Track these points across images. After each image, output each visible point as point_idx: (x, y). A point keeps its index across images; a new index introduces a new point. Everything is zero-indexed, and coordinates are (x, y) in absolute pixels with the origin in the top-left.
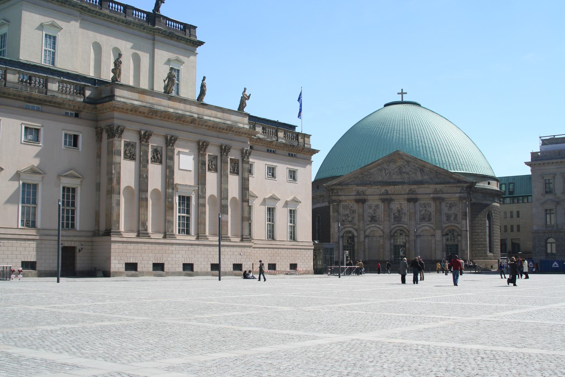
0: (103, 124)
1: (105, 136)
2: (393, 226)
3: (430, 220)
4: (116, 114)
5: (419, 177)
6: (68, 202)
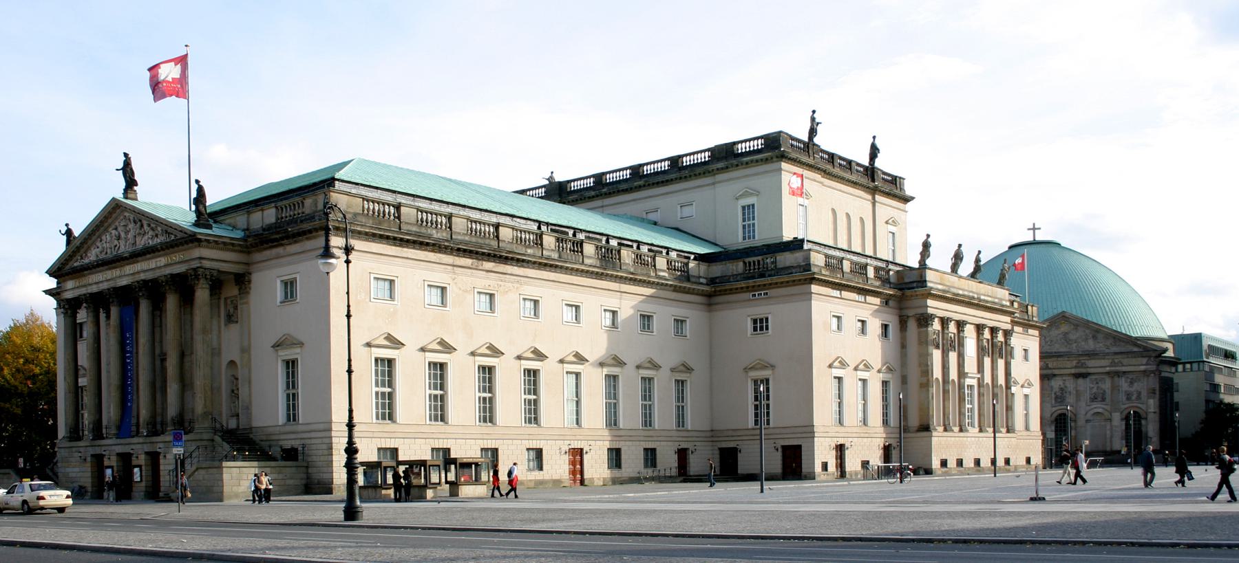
0: (911, 313)
1: (912, 325)
2: (1054, 409)
3: (1103, 400)
4: (930, 302)
5: (1091, 345)
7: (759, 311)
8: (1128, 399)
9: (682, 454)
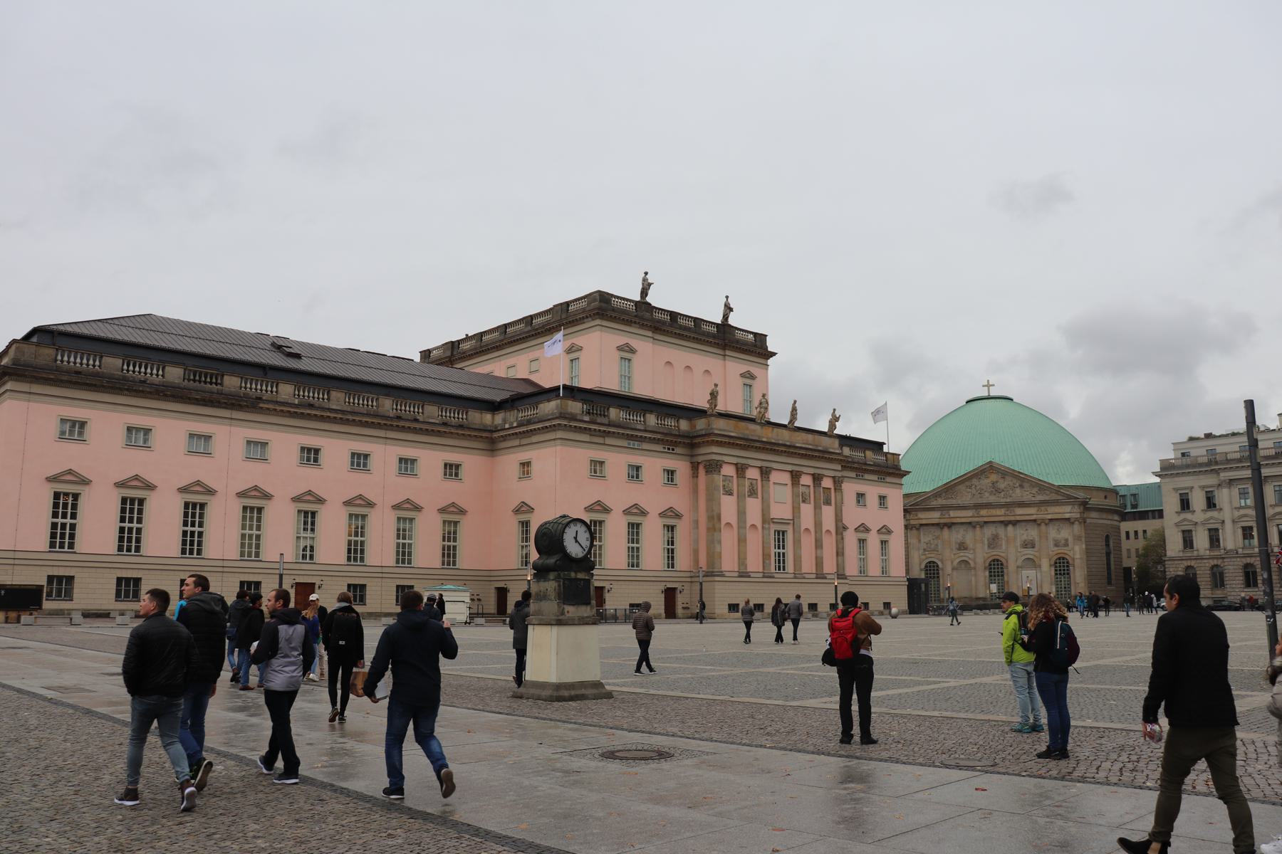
1: (702, 471)
5: (1018, 494)
7: (524, 455)
8: (1056, 545)
9: (670, 594)
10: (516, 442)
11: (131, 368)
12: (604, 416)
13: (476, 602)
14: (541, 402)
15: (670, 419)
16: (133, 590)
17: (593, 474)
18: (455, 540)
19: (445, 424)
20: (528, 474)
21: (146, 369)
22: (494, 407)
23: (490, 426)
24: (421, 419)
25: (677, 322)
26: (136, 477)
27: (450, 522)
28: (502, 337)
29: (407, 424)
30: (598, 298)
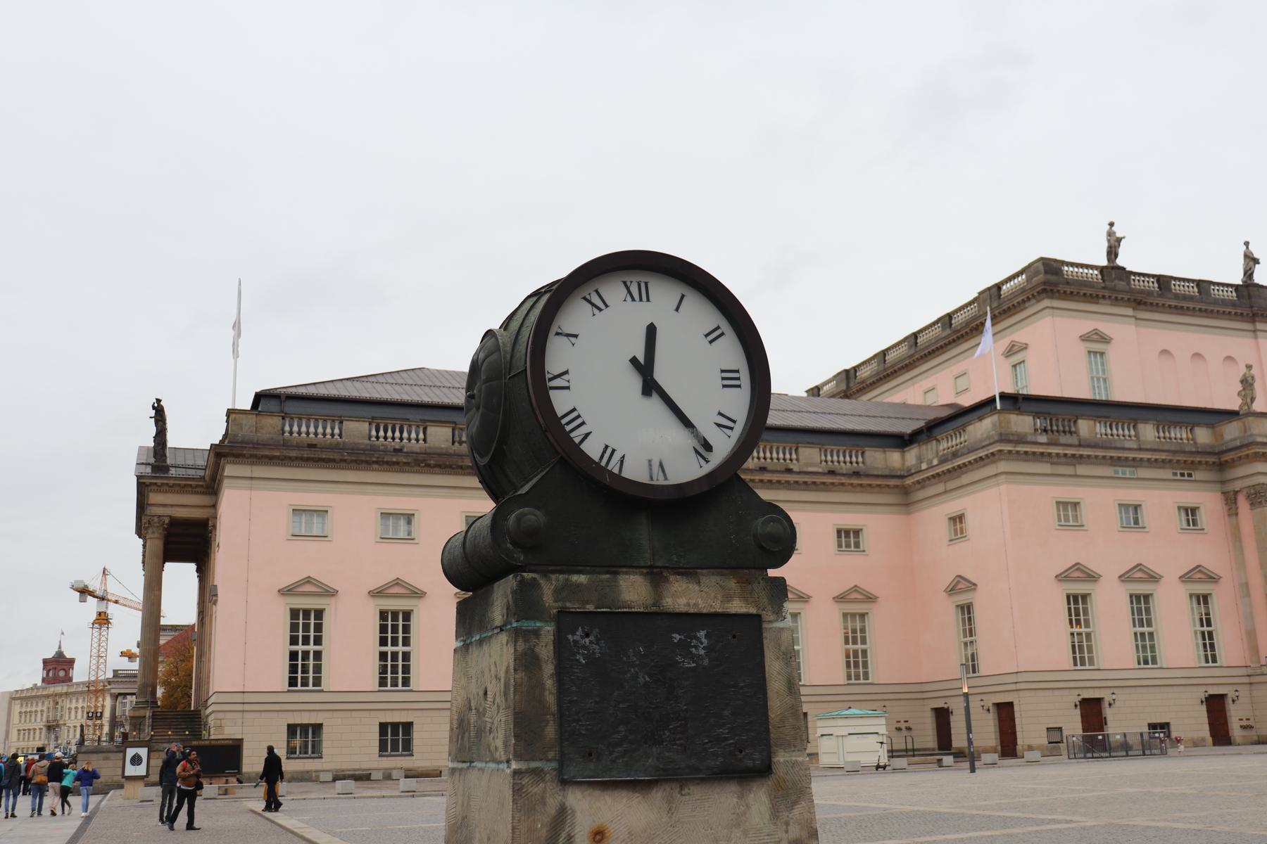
6: (1141, 621)
10: (940, 488)
11: (382, 433)
12: (1071, 432)
13: (905, 732)
14: (969, 423)
15: (1178, 428)
16: (392, 740)
17: (1063, 523)
18: (864, 641)
19: (832, 473)
20: (962, 533)
21: (401, 433)
22: (902, 441)
23: (899, 469)
24: (796, 468)
25: (1170, 290)
26: (397, 582)
27: (853, 615)
28: (912, 352)
29: (775, 477)
30: (1041, 268)
